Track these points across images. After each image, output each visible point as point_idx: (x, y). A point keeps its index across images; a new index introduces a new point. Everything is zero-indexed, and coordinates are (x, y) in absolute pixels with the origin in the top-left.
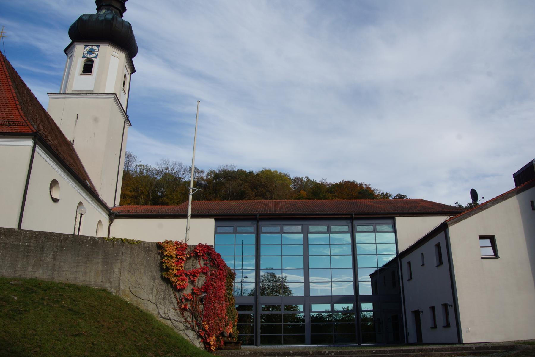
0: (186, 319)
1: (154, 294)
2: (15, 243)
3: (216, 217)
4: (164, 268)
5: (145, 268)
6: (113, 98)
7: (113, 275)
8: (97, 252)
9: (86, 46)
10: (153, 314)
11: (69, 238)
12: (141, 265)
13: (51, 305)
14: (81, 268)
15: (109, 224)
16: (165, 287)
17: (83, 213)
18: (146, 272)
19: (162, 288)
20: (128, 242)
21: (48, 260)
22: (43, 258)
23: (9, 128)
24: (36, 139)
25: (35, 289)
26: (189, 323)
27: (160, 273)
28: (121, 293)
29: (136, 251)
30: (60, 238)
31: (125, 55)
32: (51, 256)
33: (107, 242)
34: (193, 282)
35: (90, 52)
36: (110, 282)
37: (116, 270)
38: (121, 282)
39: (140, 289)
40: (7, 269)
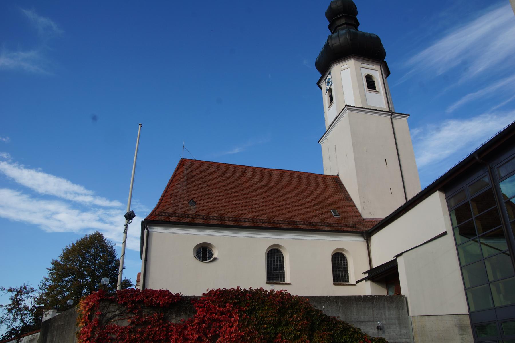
6: (347, 111)
31: (355, 59)
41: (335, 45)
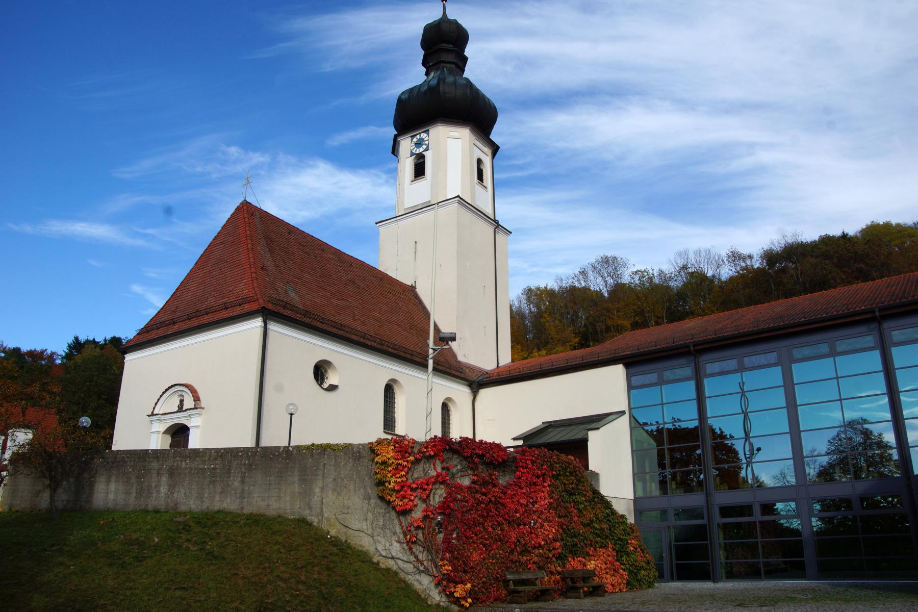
0: (416, 557)
2: (201, 466)
3: (625, 361)
5: (355, 483)
7: (314, 498)
9: (413, 137)
15: (472, 398)
16: (385, 510)
17: (293, 413)
18: (357, 489)
19: (381, 511)
21: (236, 484)
22: (231, 483)
26: (421, 563)
28: (325, 522)
29: (341, 459)
30: (248, 453)
31: (470, 130)
32: (239, 479)
33: (304, 451)
34: (425, 500)
35: (419, 144)
37: (317, 490)
38: (324, 506)
39: (349, 515)
40: (194, 500)
41: (448, 95)
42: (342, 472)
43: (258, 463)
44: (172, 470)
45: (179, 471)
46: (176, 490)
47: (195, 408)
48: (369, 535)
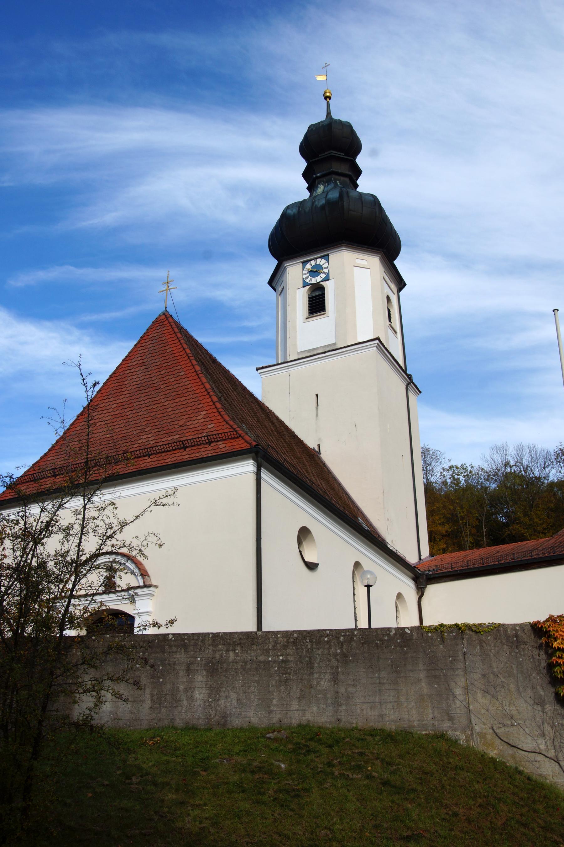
1: (548, 738)
2: (262, 658)
4: (559, 676)
5: (517, 682)
6: (375, 348)
7: (455, 703)
8: (412, 657)
9: (305, 263)
10: (556, 783)
11: (355, 636)
12: (506, 674)
13: (348, 775)
14: (387, 694)
15: (417, 598)
17: (370, 584)
20: (472, 631)
21: (325, 684)
22: (315, 683)
23: (210, 448)
24: (259, 458)
25: (312, 745)
27: (553, 690)
30: (339, 638)
31: (380, 260)
32: (328, 676)
33: (430, 635)
35: (315, 272)
36: (451, 718)
37: (458, 691)
38: (472, 715)
39: (515, 728)
40: (255, 710)
42: (494, 665)
43: (358, 651)
44: (213, 664)
45: (225, 666)
46: (222, 694)
47: (145, 586)
48: (551, 758)
